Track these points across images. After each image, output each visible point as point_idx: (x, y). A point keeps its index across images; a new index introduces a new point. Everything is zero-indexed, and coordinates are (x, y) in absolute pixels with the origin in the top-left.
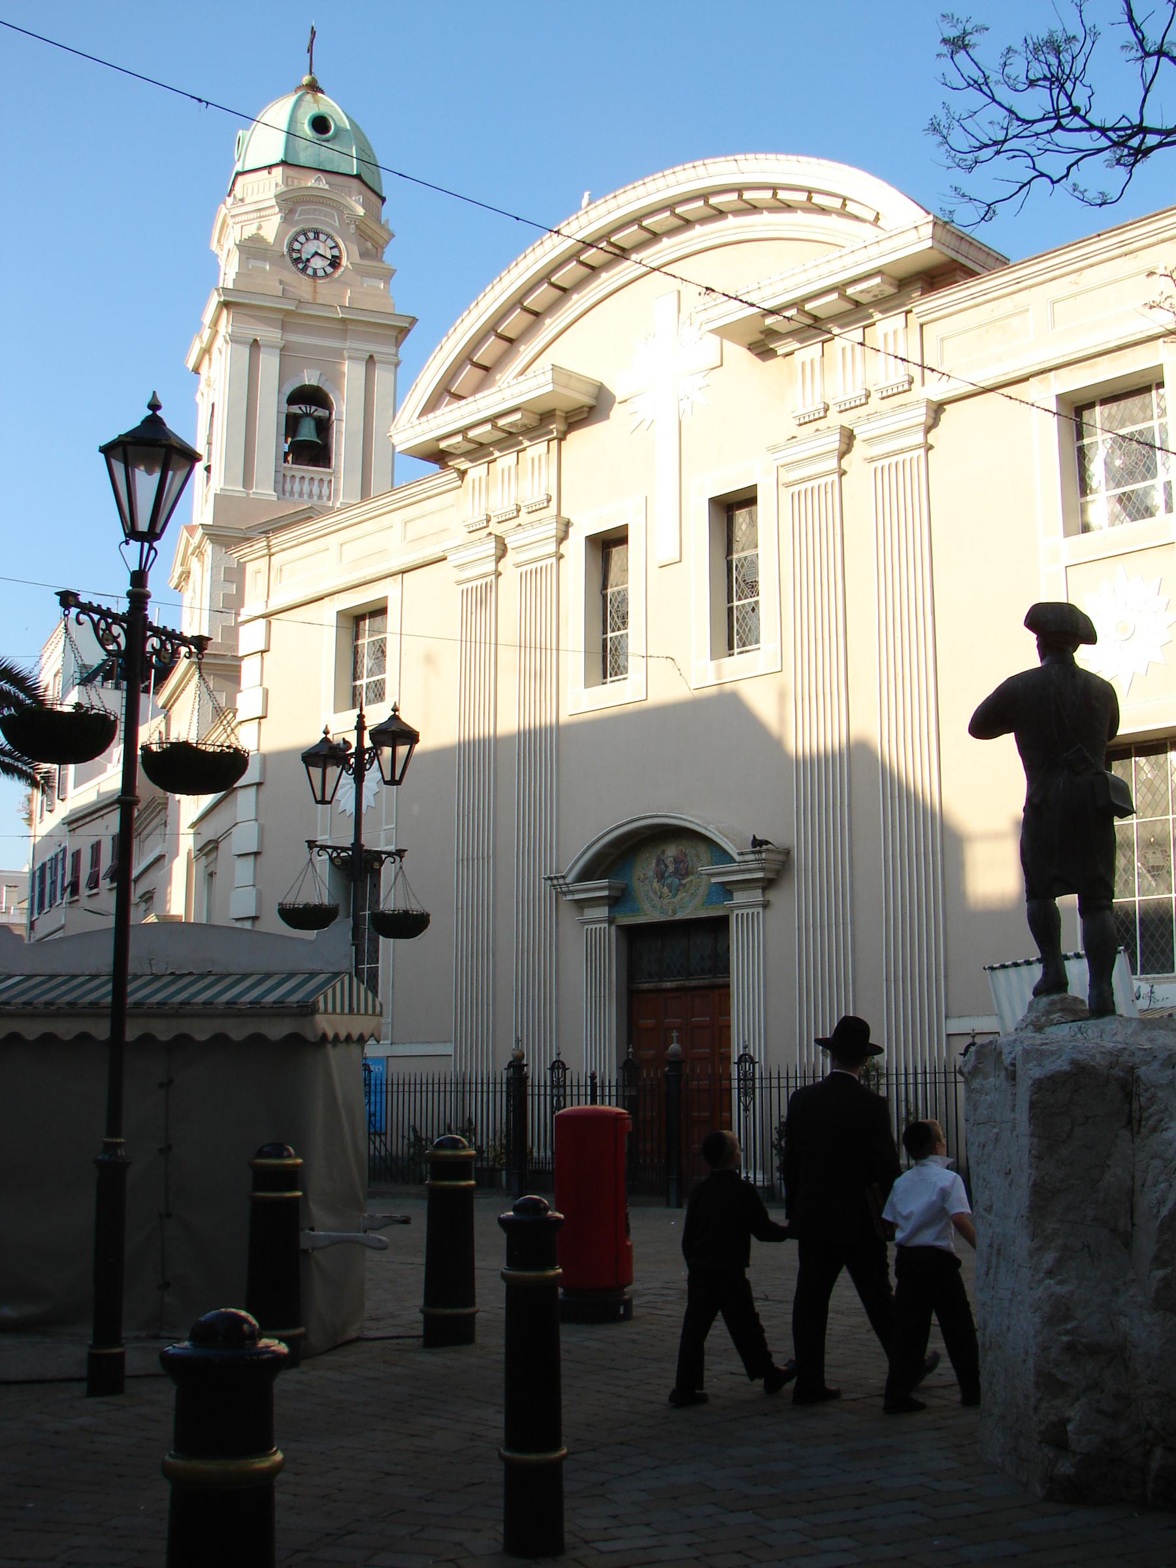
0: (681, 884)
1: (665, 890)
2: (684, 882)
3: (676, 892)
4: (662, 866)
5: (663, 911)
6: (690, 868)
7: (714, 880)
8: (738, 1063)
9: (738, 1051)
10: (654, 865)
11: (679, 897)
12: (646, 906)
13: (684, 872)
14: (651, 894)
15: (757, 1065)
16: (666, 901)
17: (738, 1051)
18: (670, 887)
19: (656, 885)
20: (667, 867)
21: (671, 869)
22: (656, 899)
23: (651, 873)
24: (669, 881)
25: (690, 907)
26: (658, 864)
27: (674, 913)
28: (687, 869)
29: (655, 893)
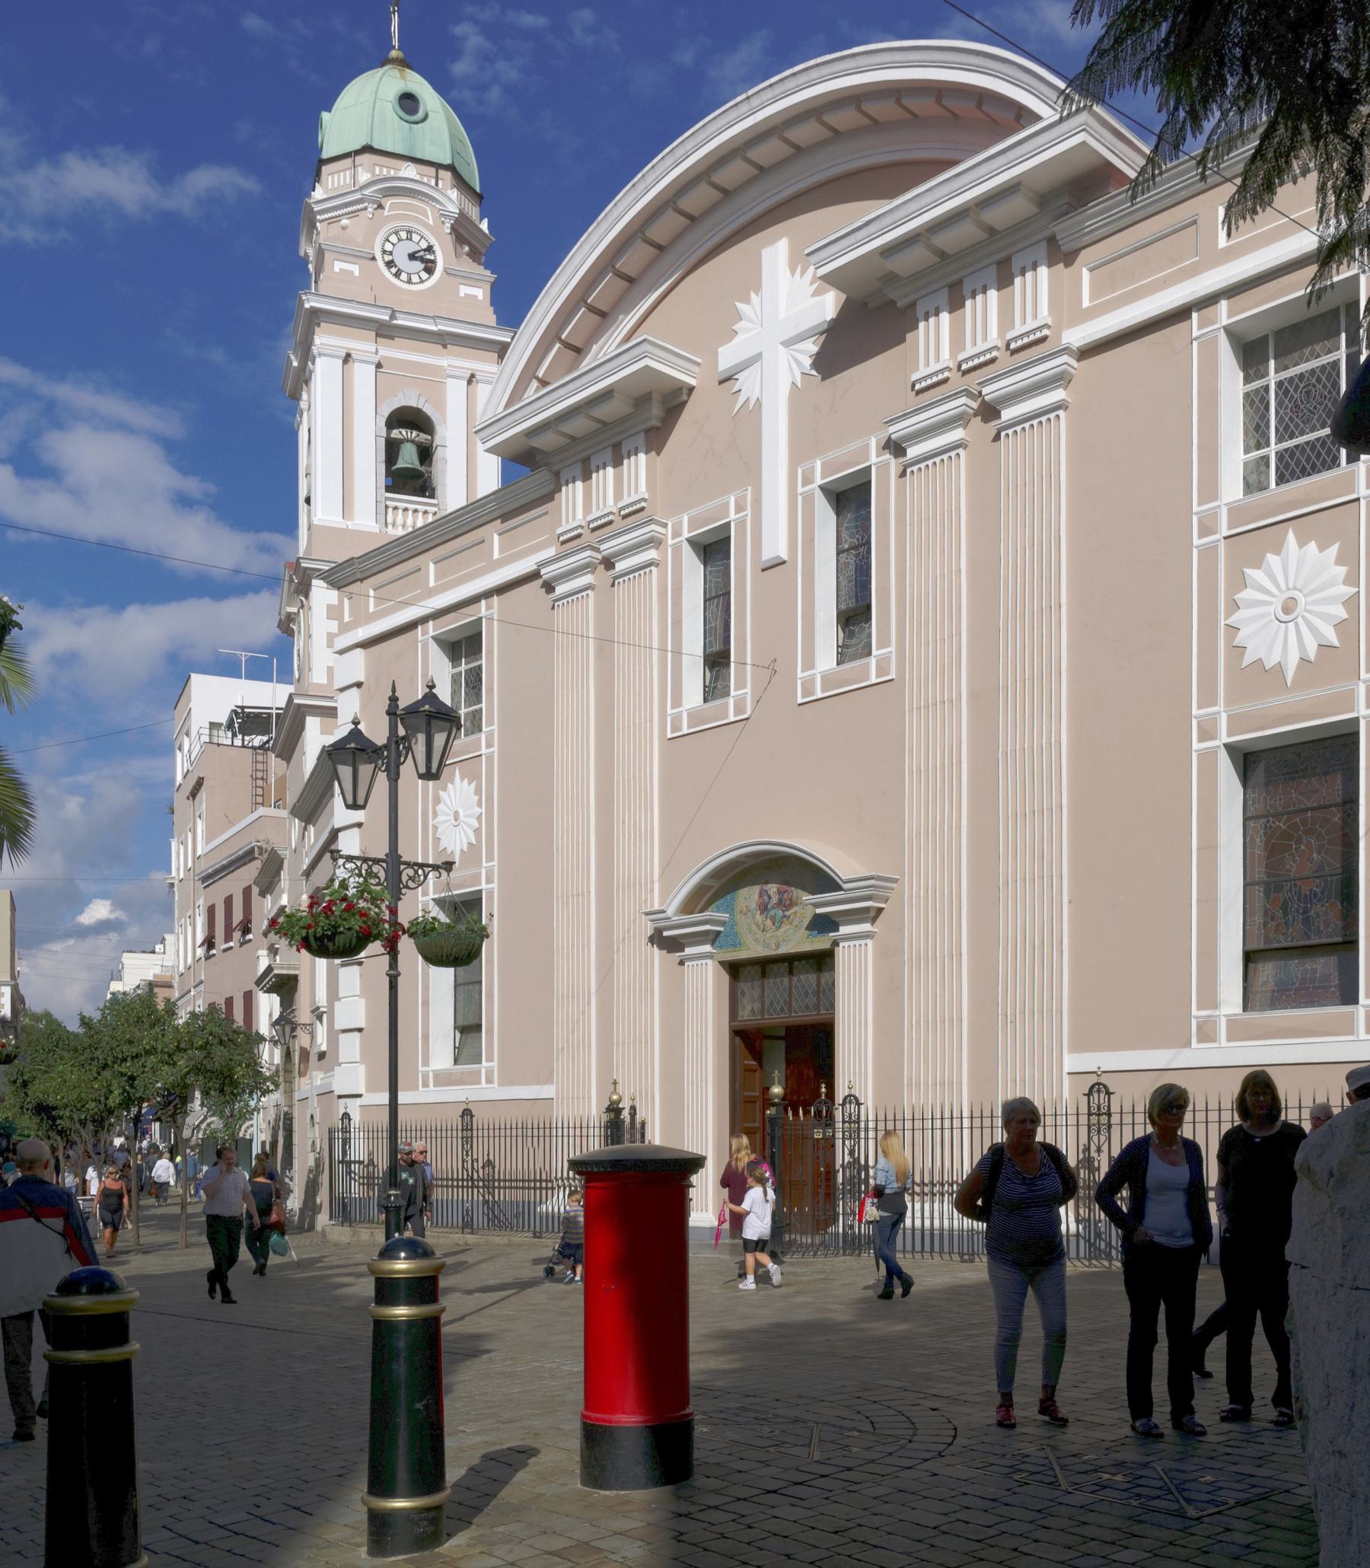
0: (784, 916)
1: (769, 922)
2: (788, 913)
3: (777, 923)
4: (766, 898)
5: (767, 946)
6: (794, 899)
7: (819, 911)
8: (843, 1105)
9: (844, 1090)
10: (756, 896)
11: (782, 930)
12: (748, 939)
13: (788, 902)
14: (754, 928)
15: (862, 1107)
16: (769, 935)
17: (844, 1090)
18: (773, 919)
19: (759, 918)
20: (770, 898)
21: (775, 900)
22: (759, 933)
23: (754, 906)
24: (772, 913)
25: (797, 941)
26: (761, 896)
27: (778, 946)
28: (791, 900)
29: (758, 925)
